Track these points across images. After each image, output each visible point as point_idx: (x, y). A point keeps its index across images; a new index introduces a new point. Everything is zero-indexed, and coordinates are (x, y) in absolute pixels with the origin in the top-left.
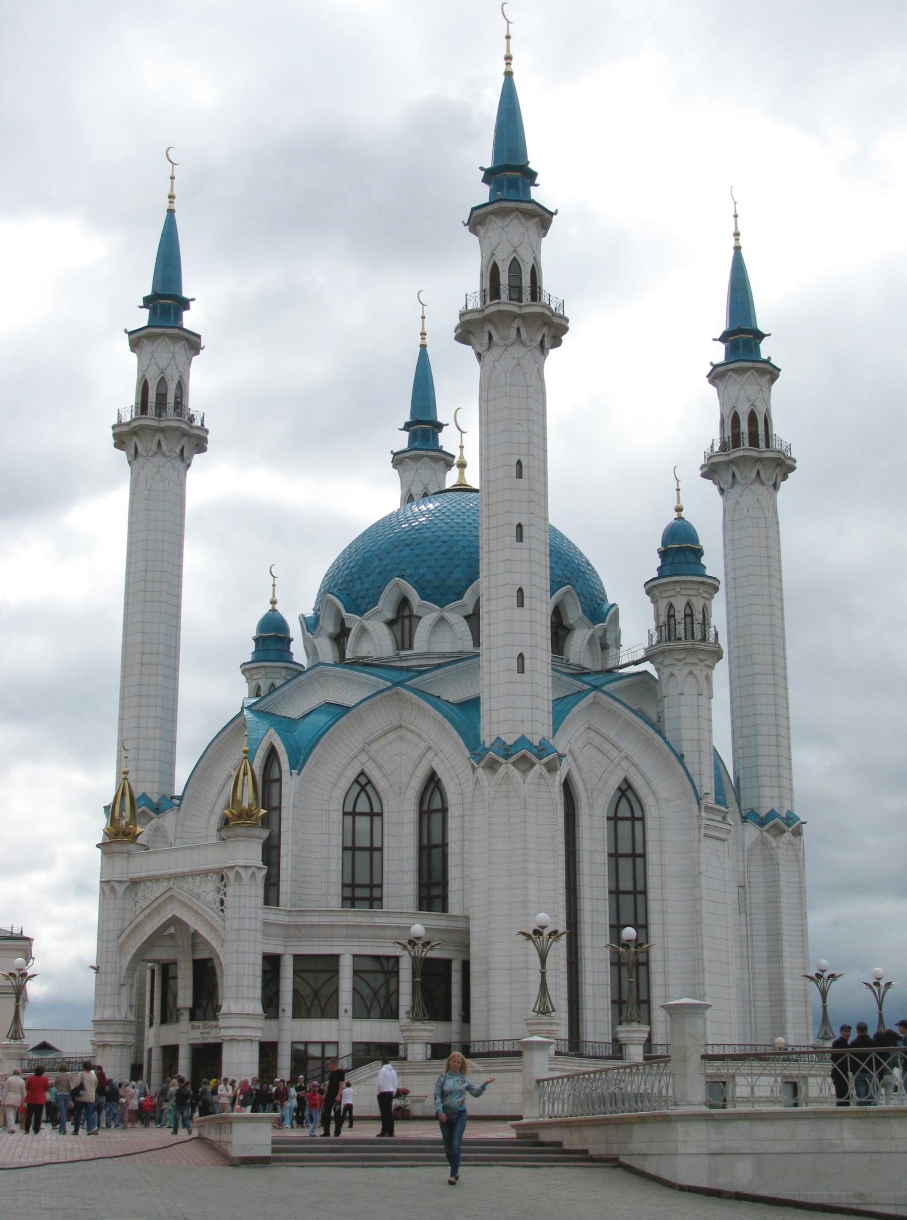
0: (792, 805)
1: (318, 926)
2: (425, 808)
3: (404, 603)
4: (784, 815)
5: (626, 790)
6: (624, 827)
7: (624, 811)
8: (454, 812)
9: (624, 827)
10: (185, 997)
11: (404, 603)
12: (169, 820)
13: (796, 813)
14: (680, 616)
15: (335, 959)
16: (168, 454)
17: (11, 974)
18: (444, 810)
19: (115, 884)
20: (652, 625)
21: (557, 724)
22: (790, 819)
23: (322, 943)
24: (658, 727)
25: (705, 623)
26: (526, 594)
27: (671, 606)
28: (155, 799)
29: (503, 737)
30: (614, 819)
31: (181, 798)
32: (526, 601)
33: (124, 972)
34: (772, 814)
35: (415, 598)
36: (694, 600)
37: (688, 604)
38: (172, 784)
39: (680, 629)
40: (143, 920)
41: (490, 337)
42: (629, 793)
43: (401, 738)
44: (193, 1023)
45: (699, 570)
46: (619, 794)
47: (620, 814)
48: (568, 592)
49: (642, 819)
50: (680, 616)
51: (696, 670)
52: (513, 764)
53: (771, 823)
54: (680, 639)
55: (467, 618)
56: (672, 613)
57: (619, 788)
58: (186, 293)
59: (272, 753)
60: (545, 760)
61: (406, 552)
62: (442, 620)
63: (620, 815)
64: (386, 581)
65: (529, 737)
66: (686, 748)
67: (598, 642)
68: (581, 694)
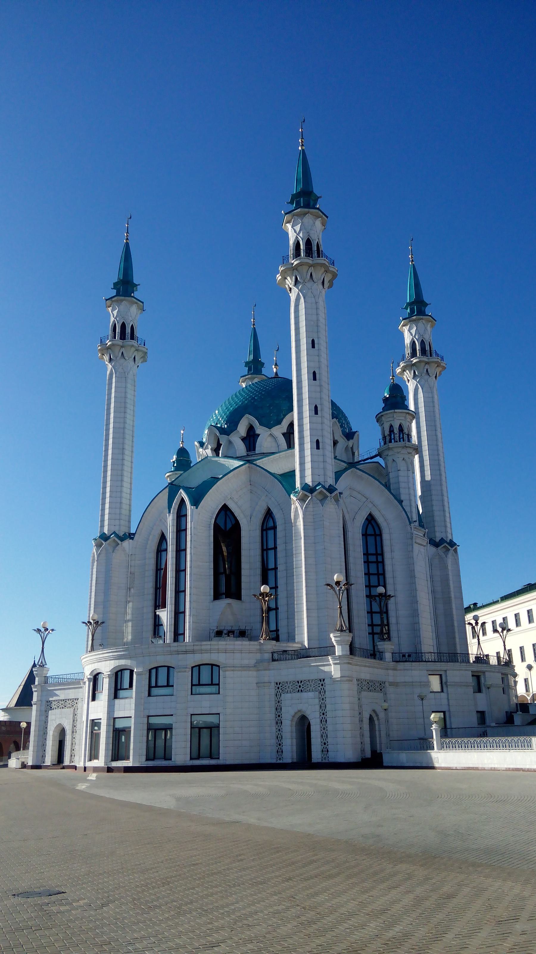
0: (452, 537)
2: (265, 528)
3: (251, 429)
4: (448, 541)
5: (371, 520)
7: (370, 531)
8: (279, 528)
9: (371, 540)
12: (127, 544)
13: (455, 540)
14: (396, 431)
16: (127, 358)
17: (38, 629)
18: (274, 528)
20: (381, 437)
21: (337, 480)
22: (452, 544)
24: (387, 486)
25: (409, 436)
27: (391, 426)
28: (121, 534)
30: (365, 535)
31: (134, 534)
32: (319, 412)
34: (442, 541)
35: (256, 424)
37: (400, 426)
38: (129, 528)
41: (296, 278)
42: (373, 522)
45: (406, 407)
46: (367, 522)
47: (368, 533)
49: (381, 535)
50: (396, 431)
52: (315, 496)
53: (443, 546)
54: (397, 442)
55: (284, 434)
56: (392, 429)
57: (367, 519)
58: (135, 281)
59: (182, 501)
60: (333, 494)
63: (368, 533)
65: (323, 483)
66: (403, 497)
67: (350, 450)
68: (346, 470)
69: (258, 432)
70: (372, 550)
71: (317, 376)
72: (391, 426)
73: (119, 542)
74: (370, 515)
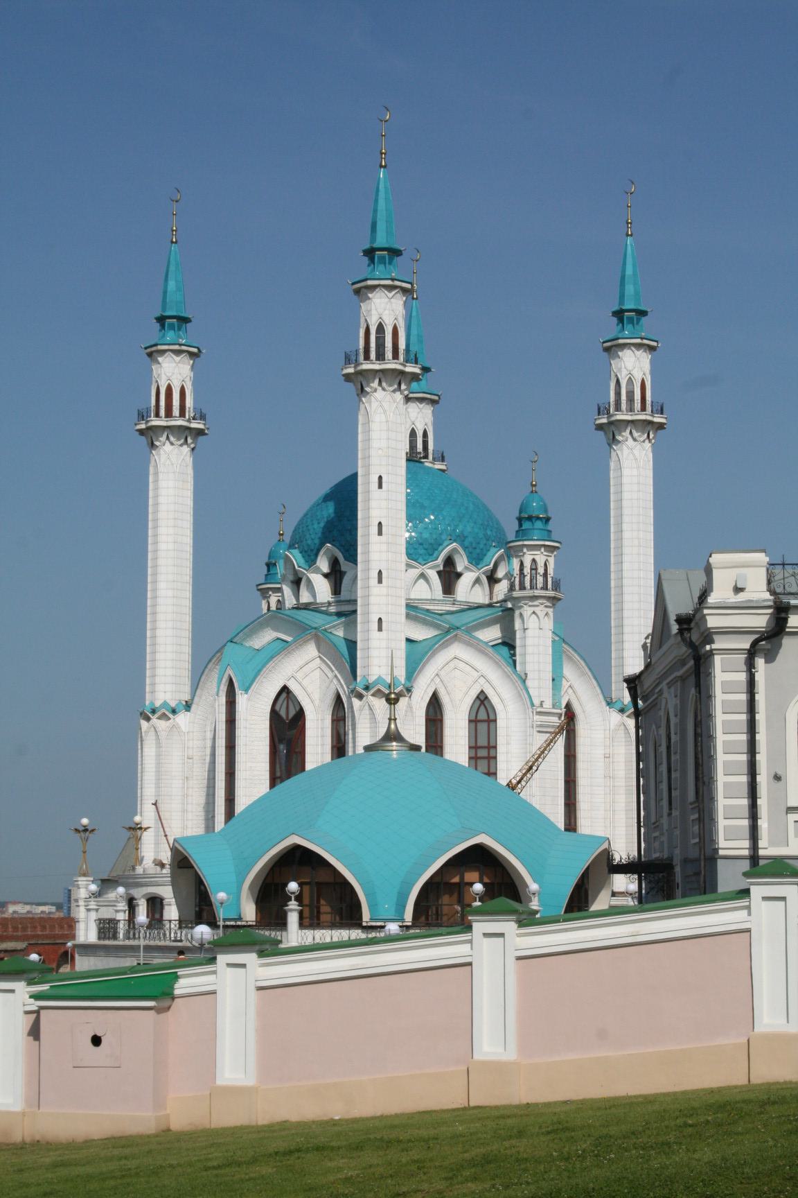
5: (482, 700)
6: (482, 727)
7: (482, 715)
9: (482, 727)
12: (182, 719)
26: (384, 575)
27: (522, 564)
30: (474, 722)
36: (537, 558)
37: (534, 560)
39: (527, 579)
46: (478, 702)
48: (455, 550)
50: (527, 570)
51: (537, 610)
66: (530, 668)
69: (343, 569)
70: (482, 741)
71: (384, 529)
72: (522, 564)
73: (171, 716)
74: (482, 691)
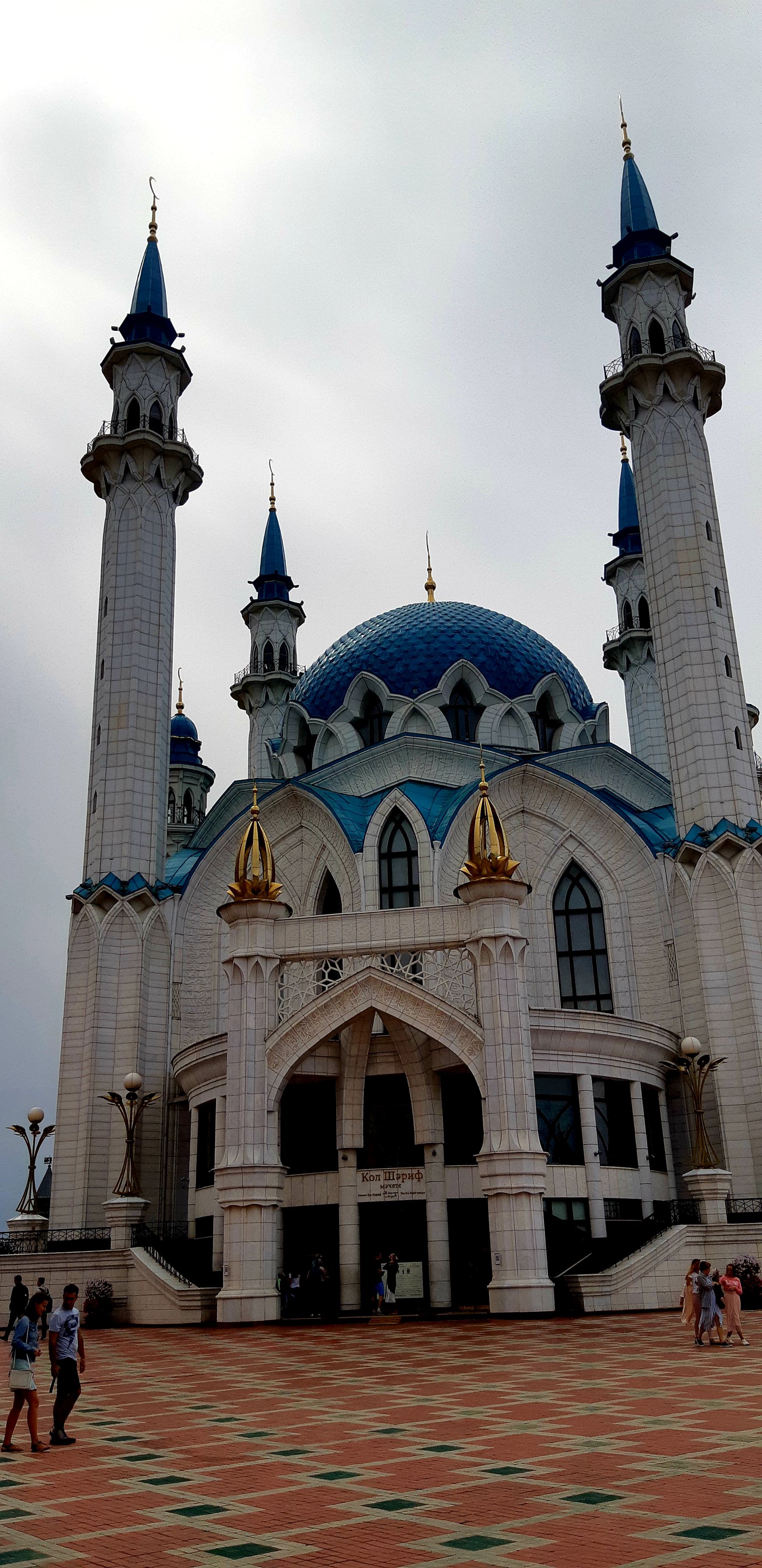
1: (562, 1033)
3: (462, 690)
8: (611, 911)
10: (351, 1132)
11: (462, 690)
15: (572, 1080)
19: (262, 962)
23: (561, 1058)
29: (732, 819)
33: (275, 1092)
40: (313, 1015)
43: (524, 825)
44: (365, 1171)
61: (458, 638)
62: (510, 713)
64: (460, 656)
